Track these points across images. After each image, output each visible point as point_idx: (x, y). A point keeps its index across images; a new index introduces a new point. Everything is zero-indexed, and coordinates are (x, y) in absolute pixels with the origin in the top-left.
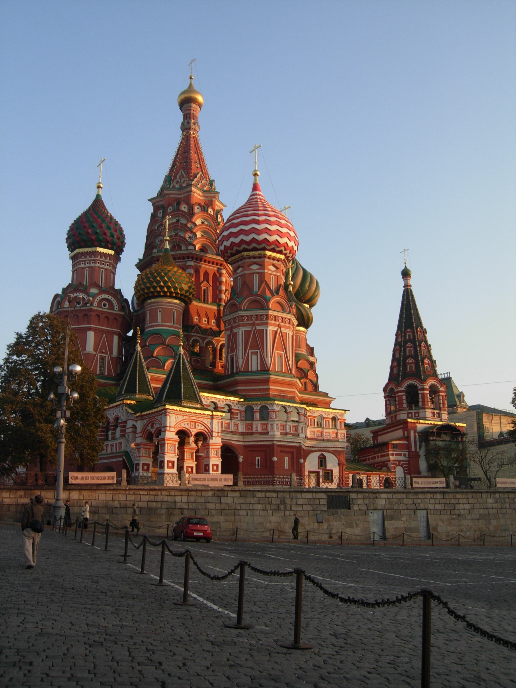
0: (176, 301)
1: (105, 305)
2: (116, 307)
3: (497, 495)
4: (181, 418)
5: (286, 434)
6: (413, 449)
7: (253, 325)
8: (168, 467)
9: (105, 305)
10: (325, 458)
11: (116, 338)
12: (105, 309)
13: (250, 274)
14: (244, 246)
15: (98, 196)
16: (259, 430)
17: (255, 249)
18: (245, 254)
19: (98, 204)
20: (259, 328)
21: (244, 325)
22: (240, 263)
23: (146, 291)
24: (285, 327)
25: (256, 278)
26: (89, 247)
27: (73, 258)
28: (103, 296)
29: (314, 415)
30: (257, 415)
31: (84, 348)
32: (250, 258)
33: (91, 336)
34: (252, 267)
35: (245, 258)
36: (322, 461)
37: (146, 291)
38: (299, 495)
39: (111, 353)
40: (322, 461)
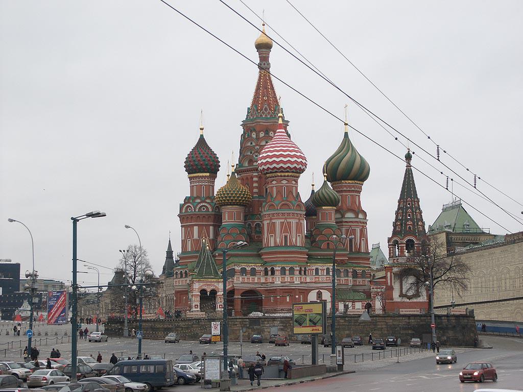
0: (237, 206)
1: (204, 209)
2: (210, 210)
3: (347, 319)
4: (202, 284)
5: (286, 282)
6: (389, 284)
7: (271, 219)
8: (195, 308)
9: (204, 209)
10: (321, 293)
11: (211, 228)
12: (204, 210)
13: (272, 187)
14: (270, 170)
15: (202, 136)
16: (270, 281)
17: (271, 173)
18: (268, 175)
19: (202, 142)
20: (273, 221)
21: (266, 220)
22: (275, 178)
23: (220, 202)
24: (289, 218)
25: (275, 189)
26: (195, 173)
27: (190, 178)
28: (202, 204)
29: (312, 268)
30: (270, 273)
31: (193, 237)
32: (271, 177)
33: (196, 228)
34: (273, 182)
35: (268, 178)
36: (319, 295)
37: (220, 202)
38: (235, 320)
39: (209, 236)
40: (319, 295)
